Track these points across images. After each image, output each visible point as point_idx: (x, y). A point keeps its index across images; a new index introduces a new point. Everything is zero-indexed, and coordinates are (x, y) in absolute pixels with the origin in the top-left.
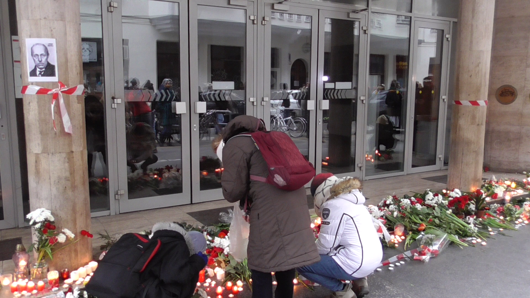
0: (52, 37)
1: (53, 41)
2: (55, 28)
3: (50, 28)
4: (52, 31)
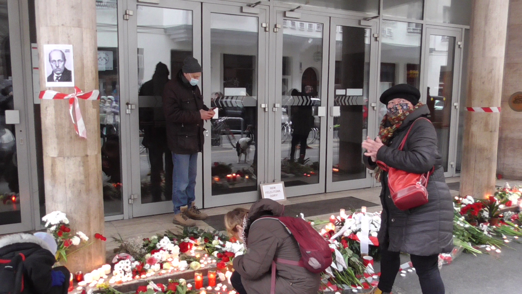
0: (69, 43)
1: (70, 47)
2: (72, 35)
3: (68, 34)
4: (69, 37)
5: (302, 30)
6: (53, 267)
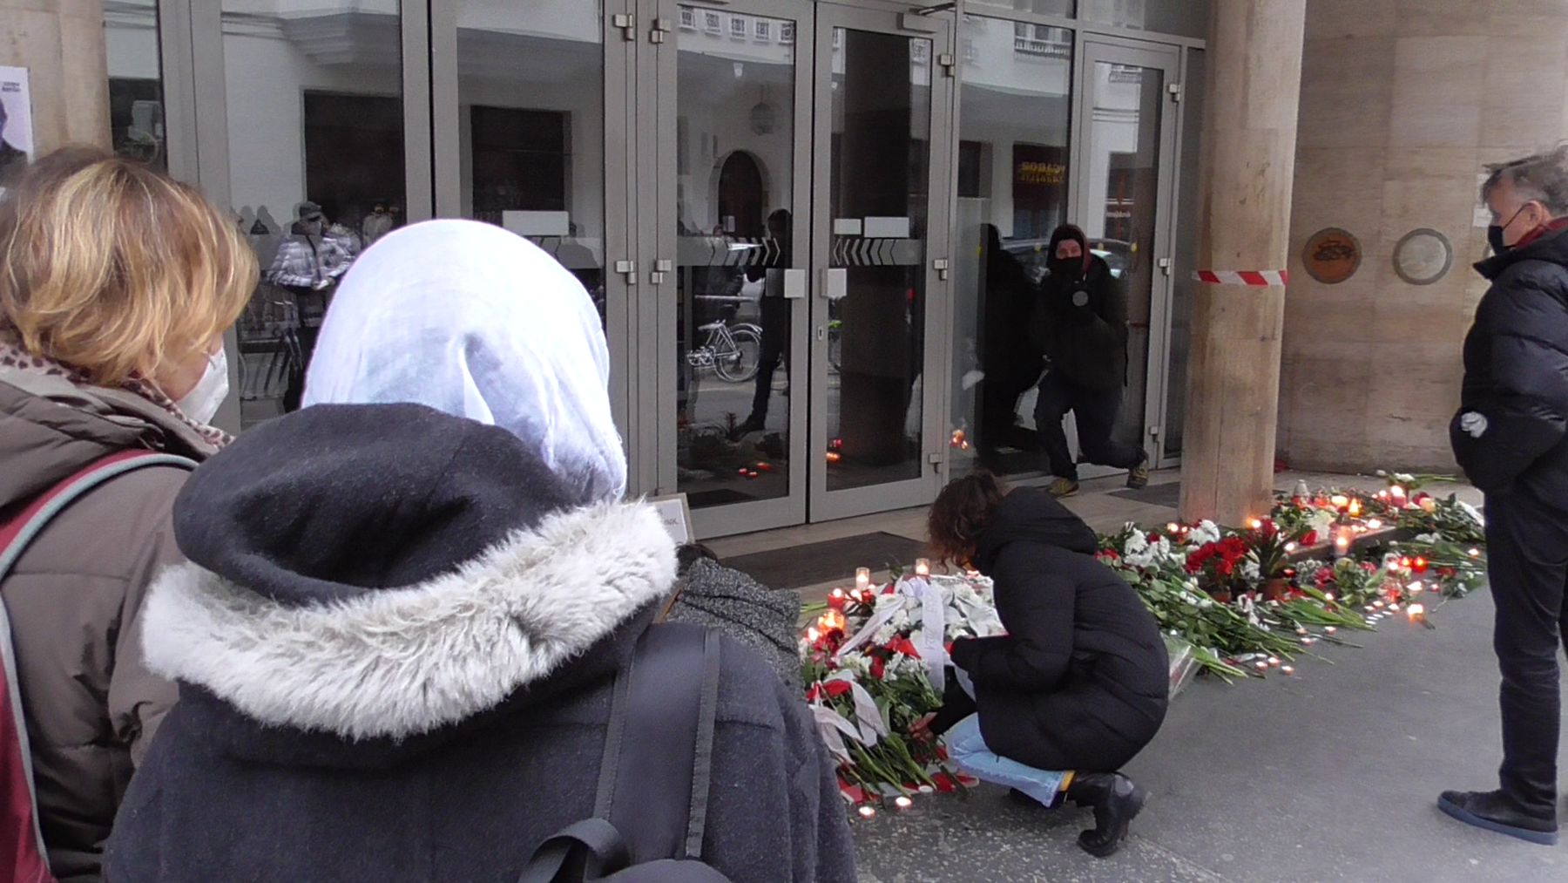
0: (16, 60)
1: (19, 75)
2: (25, 34)
3: (10, 33)
4: (14, 42)
5: (762, 41)
6: (973, 697)
